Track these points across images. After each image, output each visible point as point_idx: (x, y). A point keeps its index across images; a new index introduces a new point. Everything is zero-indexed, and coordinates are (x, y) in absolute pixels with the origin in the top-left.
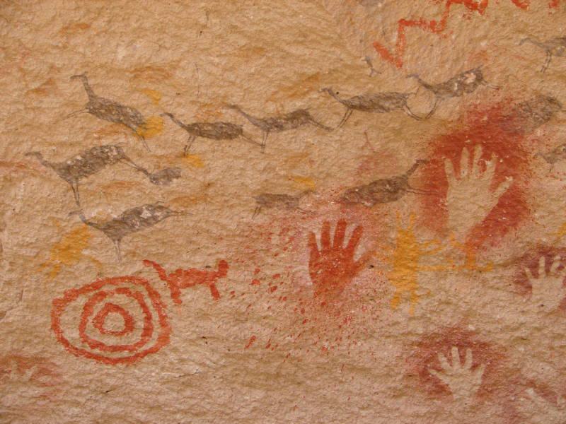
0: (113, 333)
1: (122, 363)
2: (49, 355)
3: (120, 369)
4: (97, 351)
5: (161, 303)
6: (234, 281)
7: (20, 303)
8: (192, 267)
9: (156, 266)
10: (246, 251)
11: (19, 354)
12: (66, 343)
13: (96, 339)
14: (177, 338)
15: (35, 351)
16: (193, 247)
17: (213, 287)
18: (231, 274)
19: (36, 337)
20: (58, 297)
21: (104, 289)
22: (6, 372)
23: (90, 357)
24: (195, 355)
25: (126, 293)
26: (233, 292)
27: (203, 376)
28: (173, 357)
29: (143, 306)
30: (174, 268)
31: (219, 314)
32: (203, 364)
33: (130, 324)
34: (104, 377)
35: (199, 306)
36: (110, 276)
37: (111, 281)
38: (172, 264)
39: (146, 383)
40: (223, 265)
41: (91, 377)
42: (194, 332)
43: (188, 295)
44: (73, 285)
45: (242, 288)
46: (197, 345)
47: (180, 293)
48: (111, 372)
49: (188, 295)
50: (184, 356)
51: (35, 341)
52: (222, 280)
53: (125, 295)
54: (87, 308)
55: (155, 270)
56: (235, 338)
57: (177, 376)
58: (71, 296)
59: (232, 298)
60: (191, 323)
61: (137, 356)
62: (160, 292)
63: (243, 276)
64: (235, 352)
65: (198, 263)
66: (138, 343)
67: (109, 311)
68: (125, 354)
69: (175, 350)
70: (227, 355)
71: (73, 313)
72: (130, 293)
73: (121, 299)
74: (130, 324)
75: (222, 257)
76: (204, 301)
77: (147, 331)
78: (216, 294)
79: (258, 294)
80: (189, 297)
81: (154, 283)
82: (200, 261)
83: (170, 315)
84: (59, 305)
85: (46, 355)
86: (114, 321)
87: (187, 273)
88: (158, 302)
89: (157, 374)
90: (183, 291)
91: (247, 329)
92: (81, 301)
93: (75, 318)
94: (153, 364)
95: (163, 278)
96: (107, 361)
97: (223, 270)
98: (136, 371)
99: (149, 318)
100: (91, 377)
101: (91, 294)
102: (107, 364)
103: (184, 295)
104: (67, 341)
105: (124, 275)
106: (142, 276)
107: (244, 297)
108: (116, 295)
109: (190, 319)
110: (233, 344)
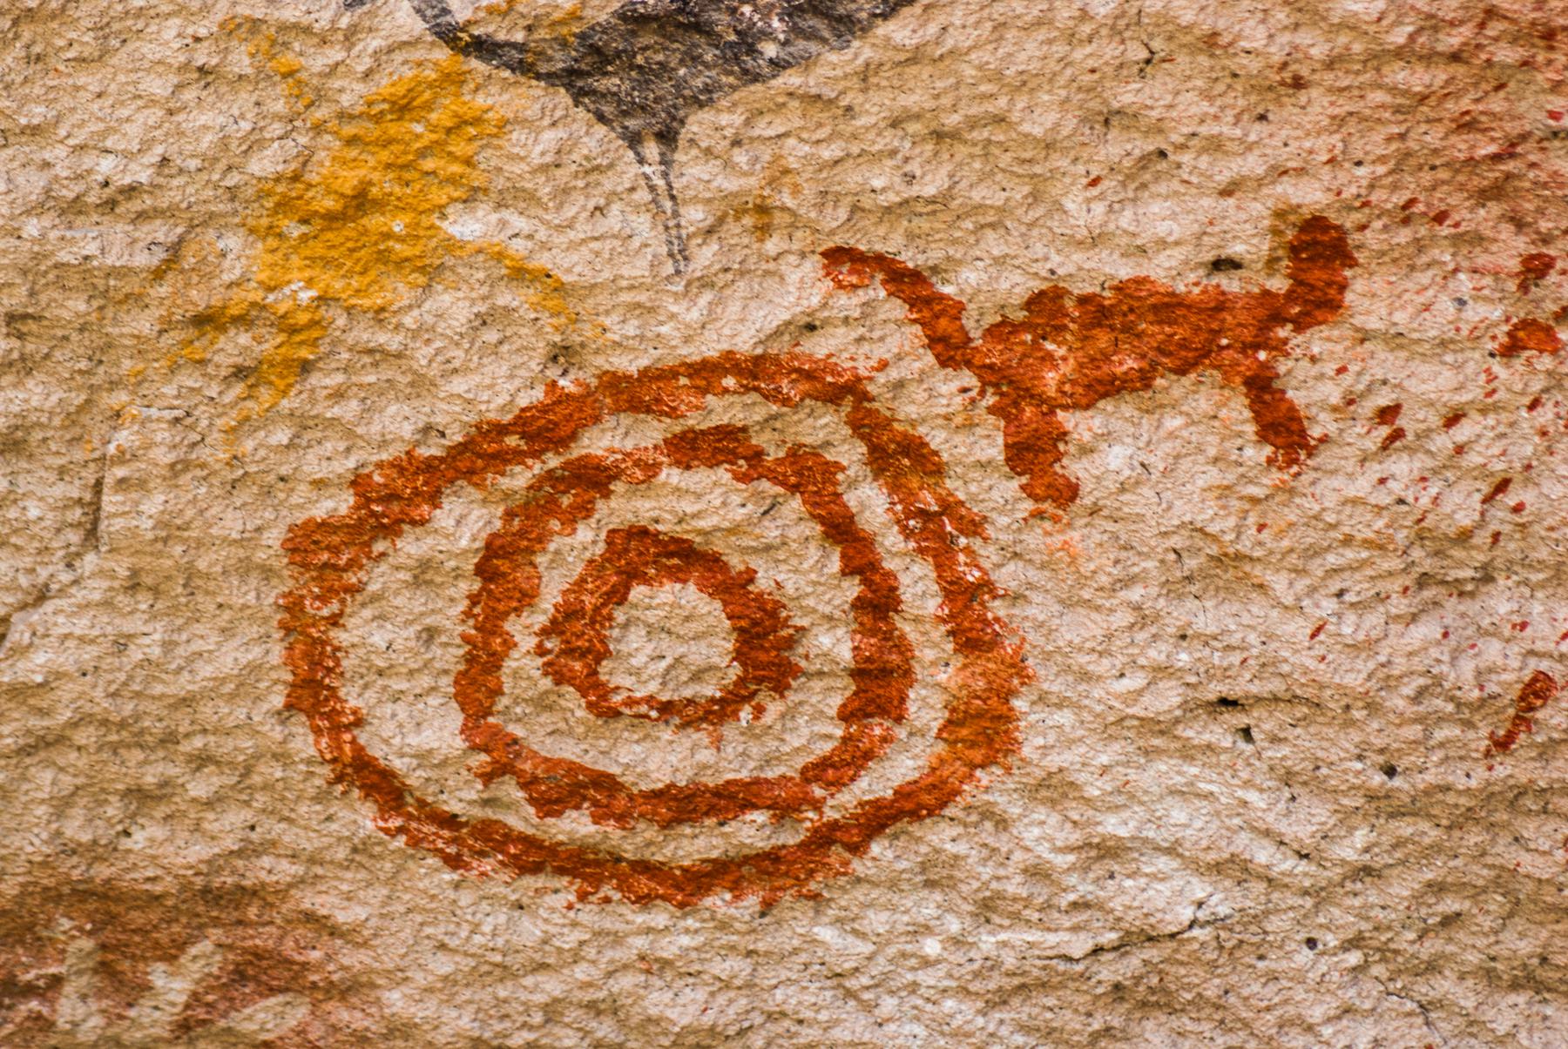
0: (667, 708)
1: (737, 889)
2: (287, 870)
3: (724, 926)
4: (576, 826)
5: (949, 507)
6: (1396, 340)
7: (90, 561)
8: (1125, 271)
9: (907, 282)
10: (1460, 146)
11: (102, 872)
12: (382, 786)
13: (569, 751)
14: (1065, 718)
15: (199, 852)
16: (1119, 147)
17: (1263, 390)
18: (1369, 297)
19: (201, 761)
20: (320, 511)
21: (601, 441)
22: (30, 990)
23: (536, 869)
24: (1179, 815)
25: (731, 457)
26: (1387, 414)
27: (1239, 941)
28: (1042, 833)
29: (841, 530)
30: (1016, 286)
31: (1314, 552)
32: (1235, 869)
33: (766, 651)
34: (626, 982)
35: (1183, 511)
36: (630, 364)
37: (631, 394)
38: (999, 261)
39: (888, 1005)
40: (1318, 254)
41: (551, 986)
42: (1162, 671)
43: (1107, 447)
44: (407, 430)
45: (1447, 378)
46: (1187, 753)
47: (1063, 435)
48: (669, 947)
49: (1107, 447)
50: (1114, 826)
51: (200, 787)
52: (1319, 340)
53: (723, 474)
54: (501, 568)
55: (897, 309)
56: (1417, 698)
57: (1079, 945)
58: (393, 499)
59: (1386, 446)
60: (1143, 618)
61: (824, 838)
62: (937, 439)
63: (1446, 306)
64: (1430, 777)
65: (1162, 244)
66: (824, 764)
67: (633, 575)
68: (752, 831)
69: (1054, 789)
70: (1381, 806)
71: (411, 603)
72: (757, 455)
73: (702, 501)
74: (766, 651)
75: (1310, 195)
76: (1213, 476)
77: (878, 687)
78: (1285, 432)
79: (1545, 415)
80: (1116, 458)
81: (900, 385)
82: (1169, 236)
83: (1007, 576)
84: (328, 559)
85: (272, 870)
86: (670, 637)
87: (1097, 312)
88: (929, 501)
89: (957, 942)
90: (1079, 424)
91: (1493, 632)
92: (463, 522)
93: (430, 635)
94: (930, 884)
95: (949, 349)
96: (644, 884)
97: (1317, 275)
98: (826, 933)
99: (878, 604)
100: (551, 986)
101: (519, 479)
102: (644, 901)
103: (1086, 451)
104: (387, 775)
105: (710, 347)
106: (818, 347)
107: (1462, 432)
108: (671, 475)
109: (1135, 594)
110: (1414, 731)
